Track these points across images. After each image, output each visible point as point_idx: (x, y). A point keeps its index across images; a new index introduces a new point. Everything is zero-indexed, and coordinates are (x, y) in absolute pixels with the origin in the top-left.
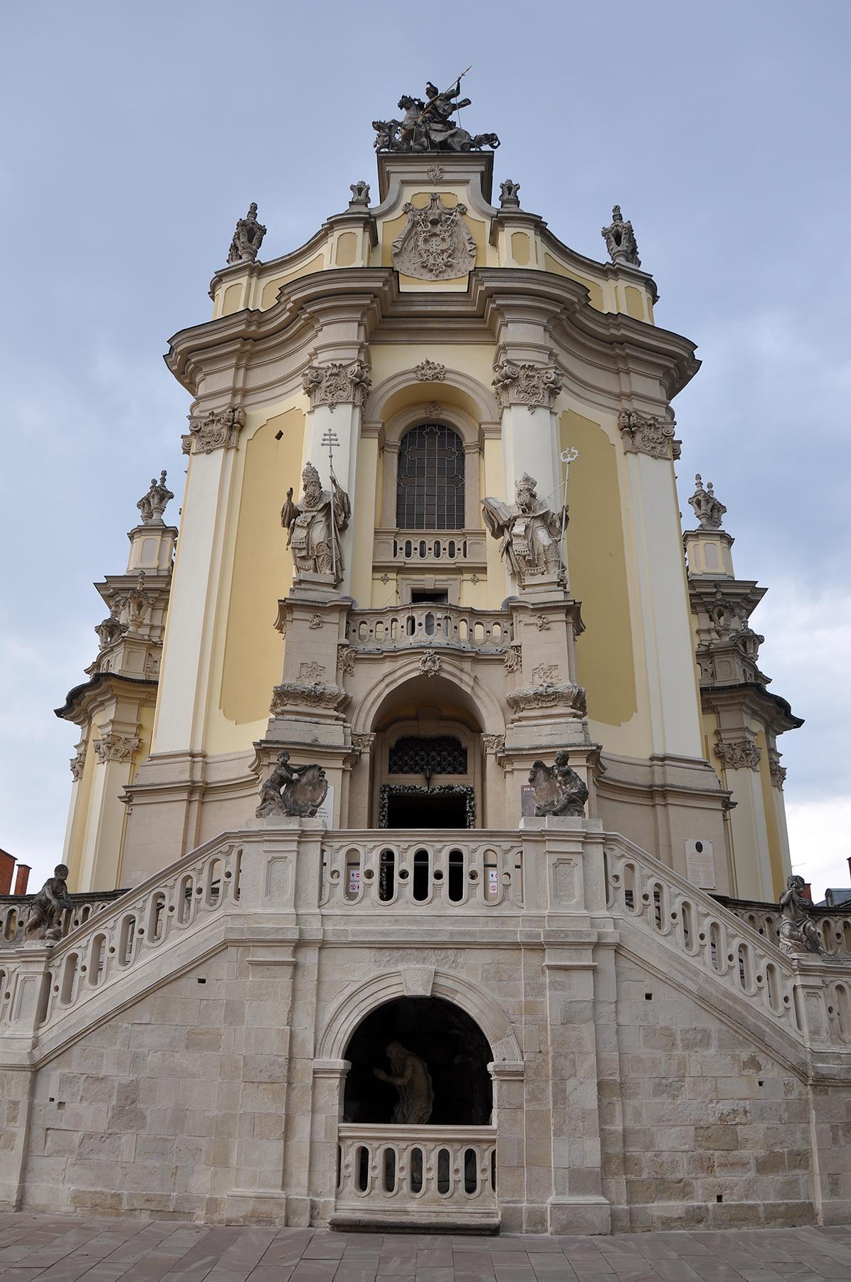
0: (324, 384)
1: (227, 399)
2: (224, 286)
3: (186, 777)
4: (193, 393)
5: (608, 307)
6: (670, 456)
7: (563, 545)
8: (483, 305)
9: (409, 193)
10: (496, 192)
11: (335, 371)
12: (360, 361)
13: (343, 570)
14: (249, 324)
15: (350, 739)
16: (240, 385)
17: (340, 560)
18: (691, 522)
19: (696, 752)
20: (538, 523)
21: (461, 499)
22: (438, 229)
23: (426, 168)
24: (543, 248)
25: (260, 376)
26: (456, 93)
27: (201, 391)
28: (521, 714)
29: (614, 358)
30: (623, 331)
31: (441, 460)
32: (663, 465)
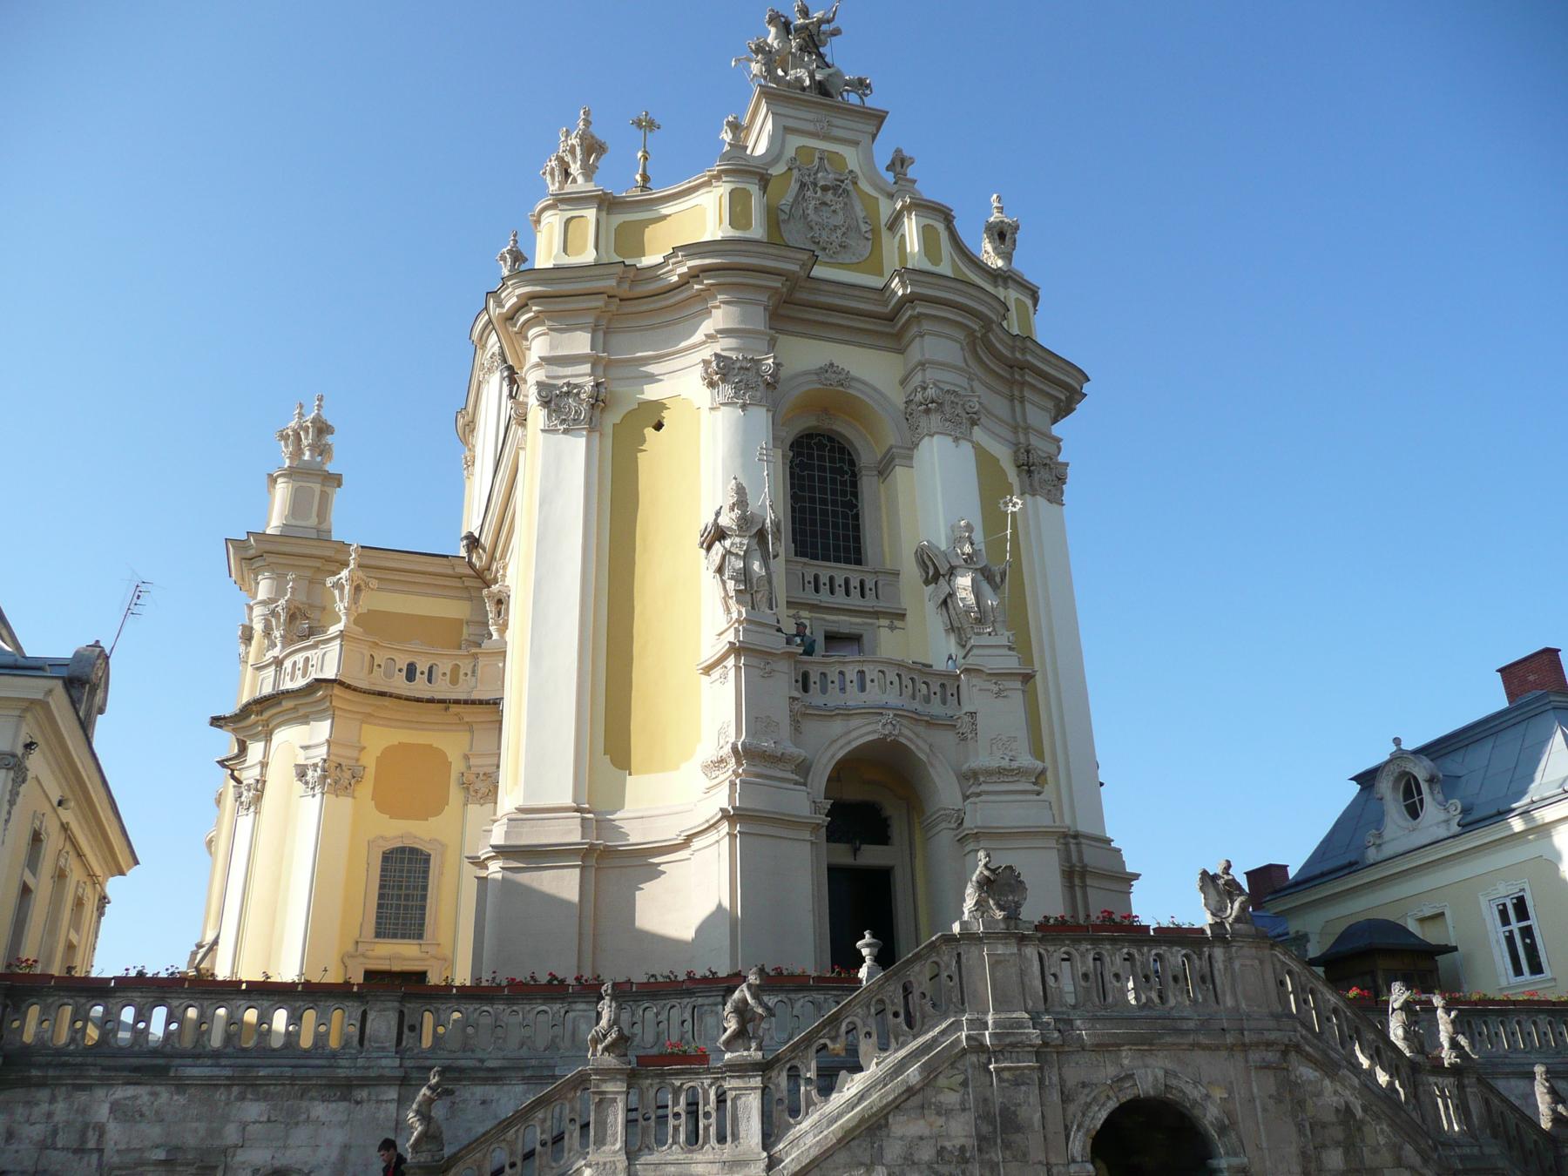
21: (857, 528)
23: (810, 116)
28: (984, 787)
29: (1011, 383)
31: (833, 481)
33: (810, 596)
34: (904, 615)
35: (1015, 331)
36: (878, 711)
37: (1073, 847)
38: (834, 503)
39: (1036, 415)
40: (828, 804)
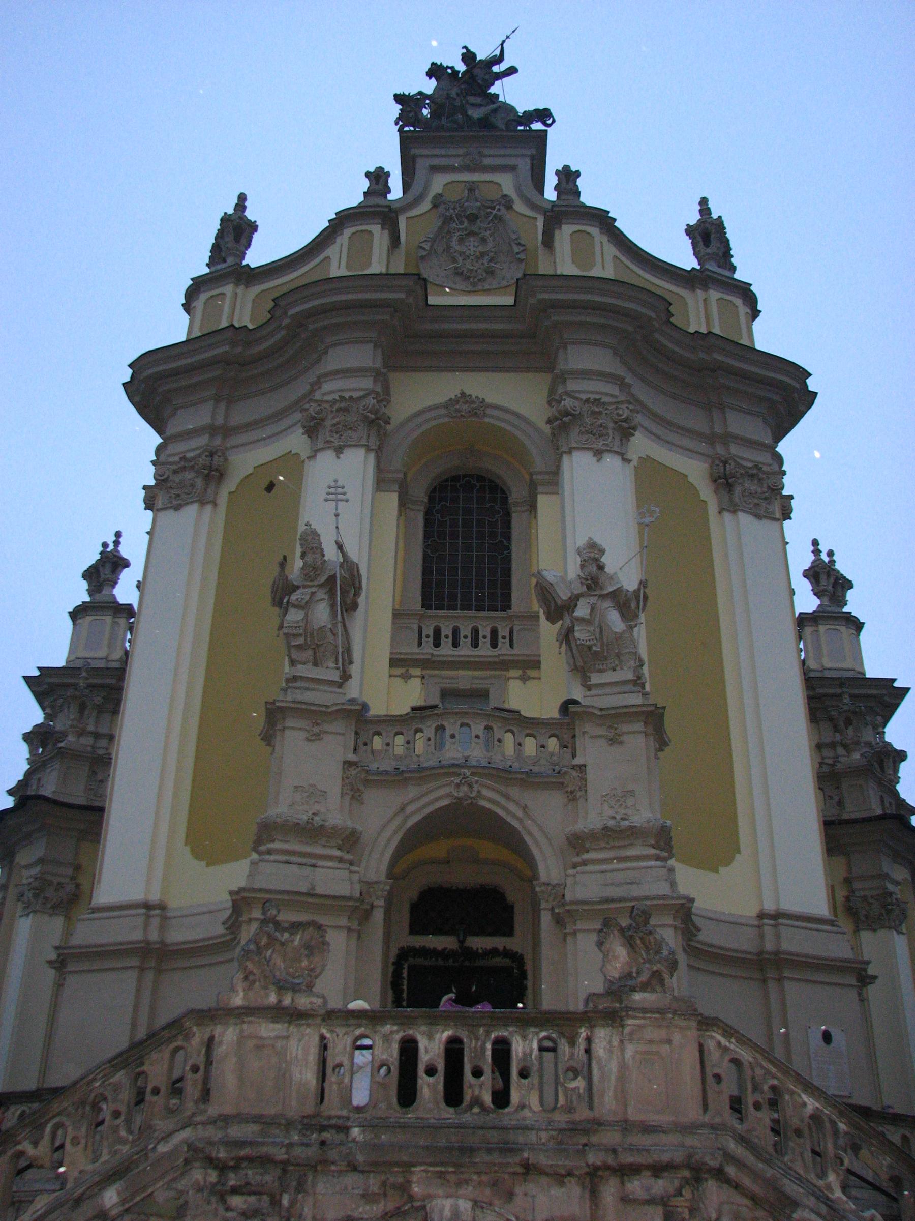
0: (328, 423)
1: (203, 440)
2: (203, 297)
3: (137, 935)
4: (159, 431)
5: (696, 325)
6: (778, 515)
7: (641, 634)
9: (438, 183)
10: (551, 180)
11: (343, 405)
12: (377, 393)
13: (351, 663)
15: (357, 887)
16: (220, 421)
17: (348, 651)
18: (806, 601)
19: (820, 906)
20: (607, 604)
21: (507, 573)
23: (461, 151)
24: (611, 250)
27: (170, 431)
28: (586, 856)
30: (716, 356)
32: (767, 526)
34: (539, 662)
35: (691, 330)
36: (452, 769)
39: (744, 425)
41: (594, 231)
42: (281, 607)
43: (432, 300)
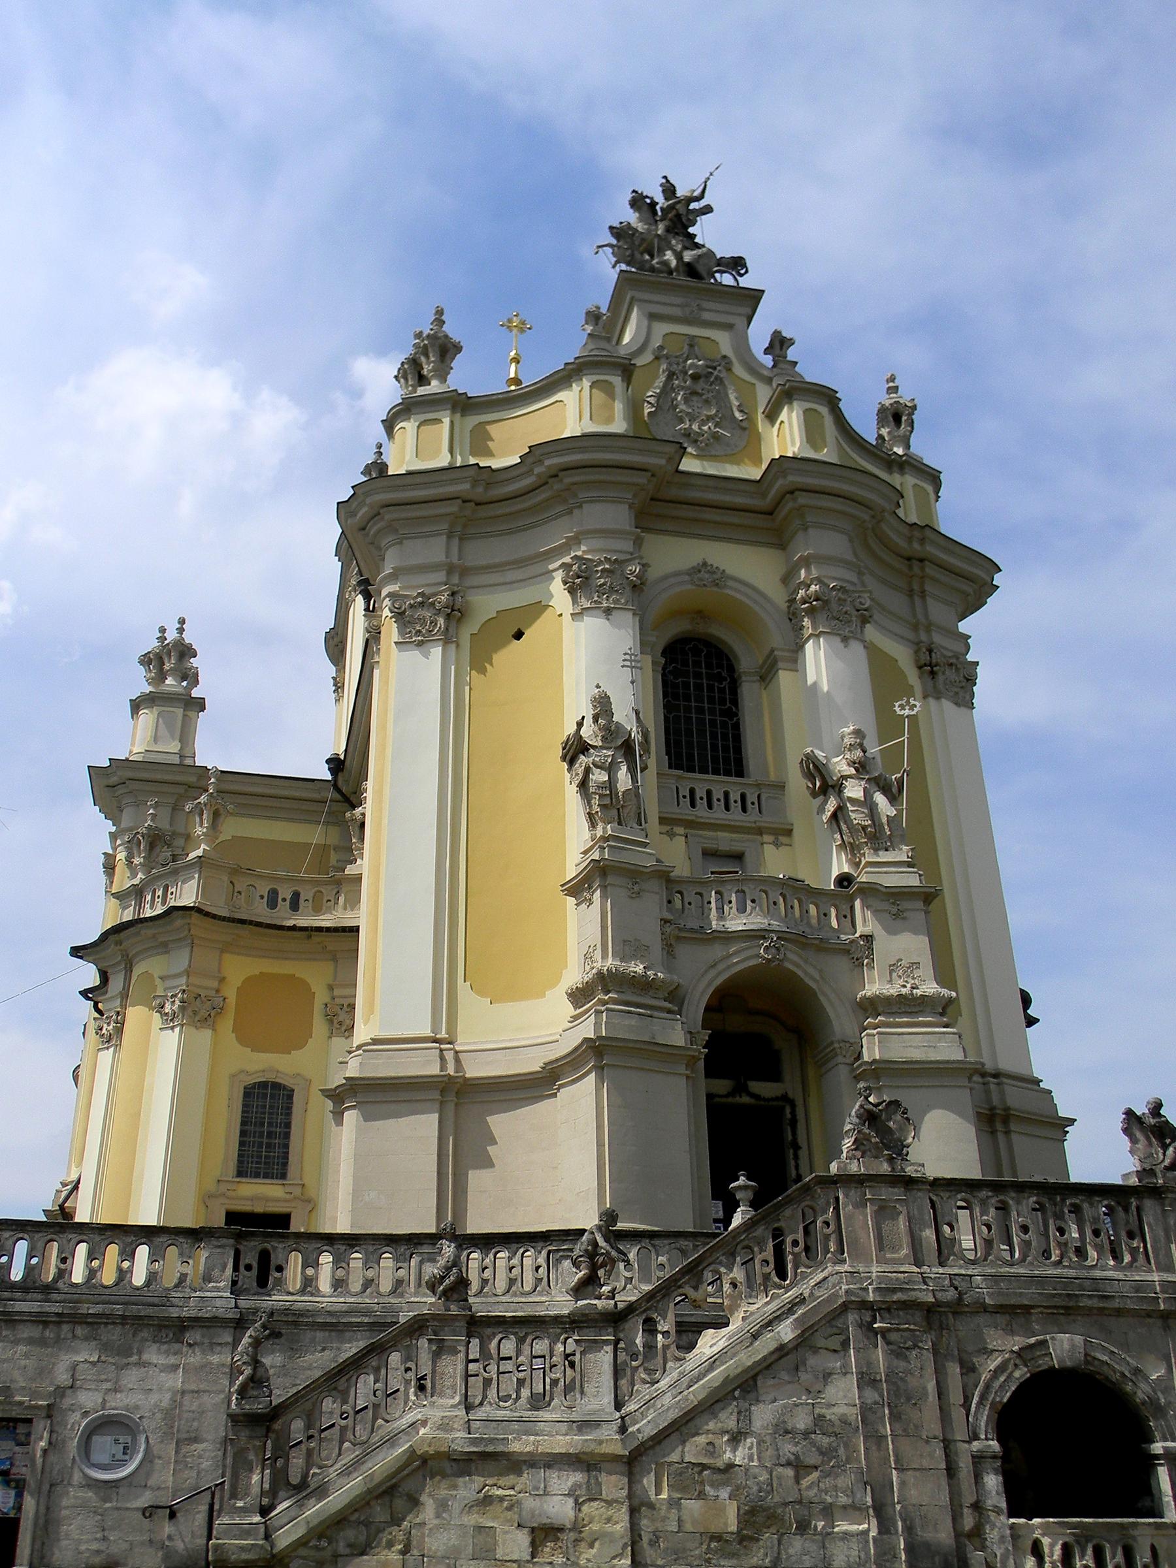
8: (778, 503)
14: (475, 483)
16: (455, 561)
21: (737, 738)
22: (700, 386)
25: (480, 552)
26: (702, 196)
31: (711, 688)
33: (686, 812)
37: (992, 1087)
38: (712, 712)
39: (938, 611)
40: (705, 1035)
41: (824, 410)
42: (571, 763)
43: (683, 467)
